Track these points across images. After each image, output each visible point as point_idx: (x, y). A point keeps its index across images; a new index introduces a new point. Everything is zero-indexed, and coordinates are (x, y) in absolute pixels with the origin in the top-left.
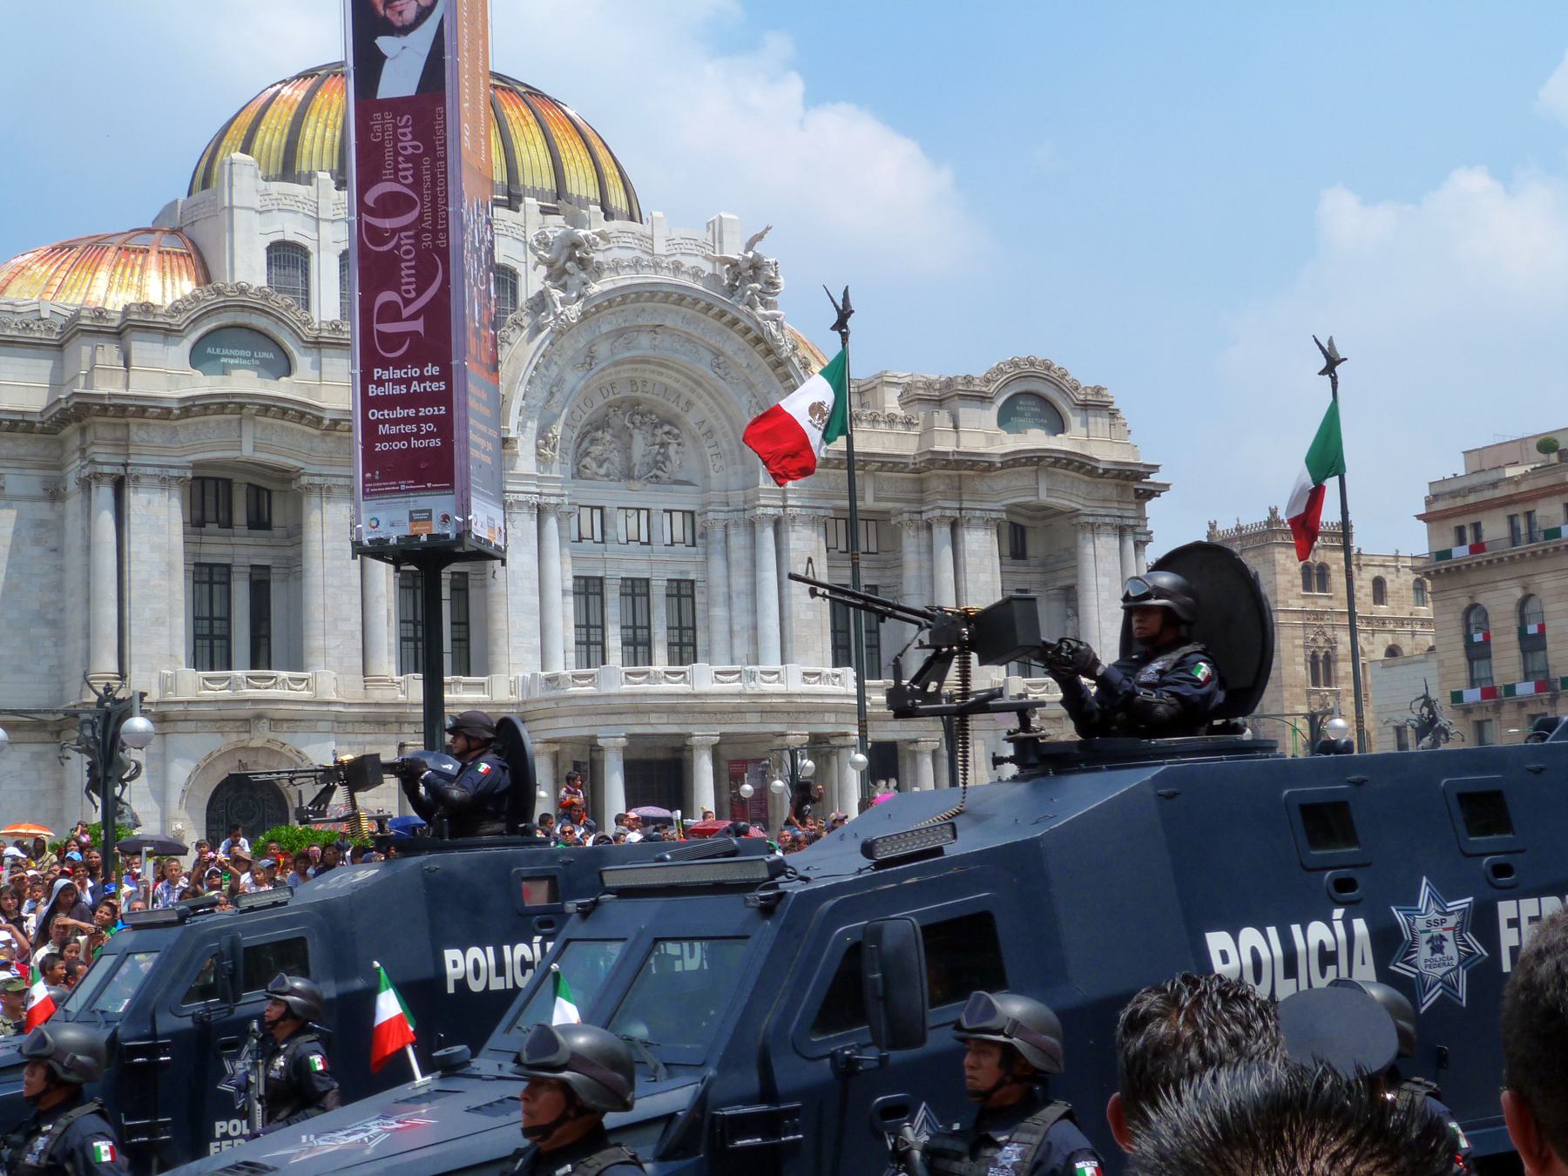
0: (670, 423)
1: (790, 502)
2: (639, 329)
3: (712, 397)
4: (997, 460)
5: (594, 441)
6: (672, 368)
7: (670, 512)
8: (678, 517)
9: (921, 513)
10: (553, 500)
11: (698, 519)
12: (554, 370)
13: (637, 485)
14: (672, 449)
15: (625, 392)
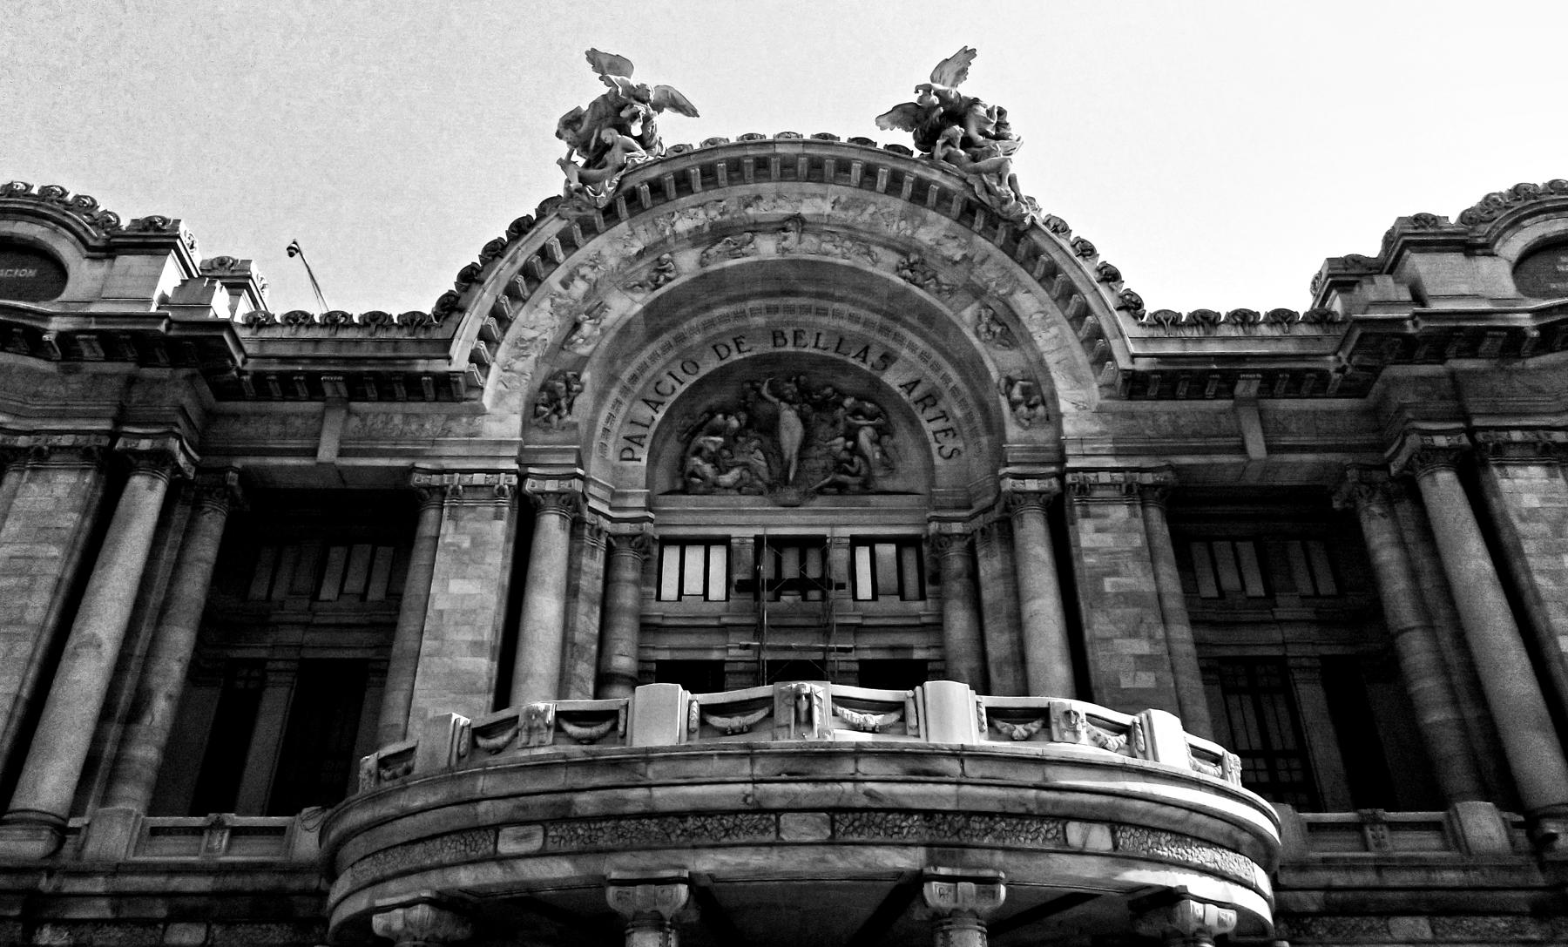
0: (860, 398)
1: (1071, 464)
2: (757, 228)
3: (923, 336)
4: (1525, 321)
5: (715, 433)
6: (841, 300)
7: (870, 541)
8: (887, 551)
9: (1385, 467)
10: (551, 486)
11: (925, 549)
12: (580, 287)
13: (791, 495)
14: (864, 437)
15: (764, 348)
